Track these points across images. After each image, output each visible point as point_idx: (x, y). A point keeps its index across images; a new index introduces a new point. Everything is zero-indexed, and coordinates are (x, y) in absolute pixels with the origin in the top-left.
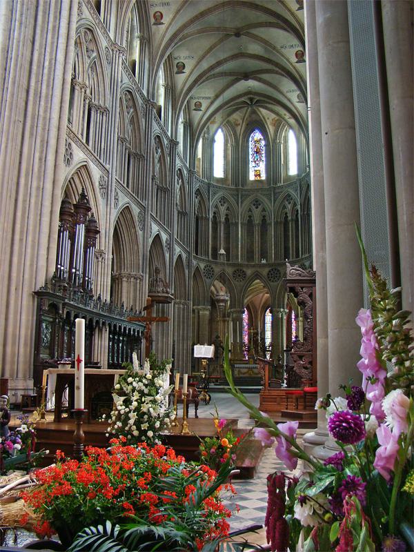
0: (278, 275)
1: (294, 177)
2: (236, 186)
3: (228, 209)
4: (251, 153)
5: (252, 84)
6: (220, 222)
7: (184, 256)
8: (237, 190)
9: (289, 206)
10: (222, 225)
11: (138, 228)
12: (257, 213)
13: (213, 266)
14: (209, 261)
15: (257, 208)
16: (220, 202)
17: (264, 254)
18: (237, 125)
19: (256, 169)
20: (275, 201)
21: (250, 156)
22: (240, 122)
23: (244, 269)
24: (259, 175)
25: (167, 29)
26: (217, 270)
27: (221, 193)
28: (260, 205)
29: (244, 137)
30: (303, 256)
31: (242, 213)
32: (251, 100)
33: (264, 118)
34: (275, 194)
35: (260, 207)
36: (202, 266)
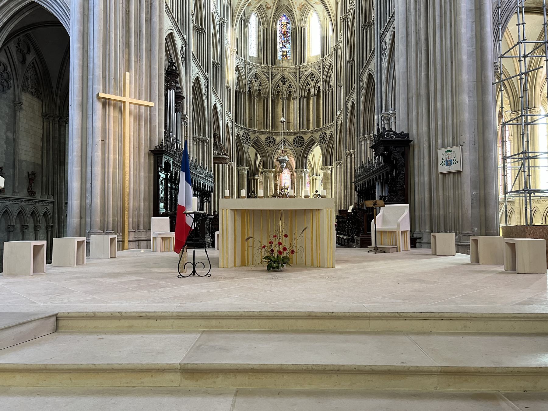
0: (302, 142)
1: (317, 56)
2: (267, 64)
3: (260, 84)
6: (254, 95)
7: (230, 124)
9: (312, 83)
11: (204, 97)
12: (284, 88)
14: (246, 129)
15: (284, 84)
18: (268, 8)
19: (283, 49)
21: (278, 38)
22: (271, 5)
23: (275, 137)
26: (253, 136)
27: (255, 70)
28: (287, 81)
29: (273, 20)
35: (287, 83)
36: (241, 133)
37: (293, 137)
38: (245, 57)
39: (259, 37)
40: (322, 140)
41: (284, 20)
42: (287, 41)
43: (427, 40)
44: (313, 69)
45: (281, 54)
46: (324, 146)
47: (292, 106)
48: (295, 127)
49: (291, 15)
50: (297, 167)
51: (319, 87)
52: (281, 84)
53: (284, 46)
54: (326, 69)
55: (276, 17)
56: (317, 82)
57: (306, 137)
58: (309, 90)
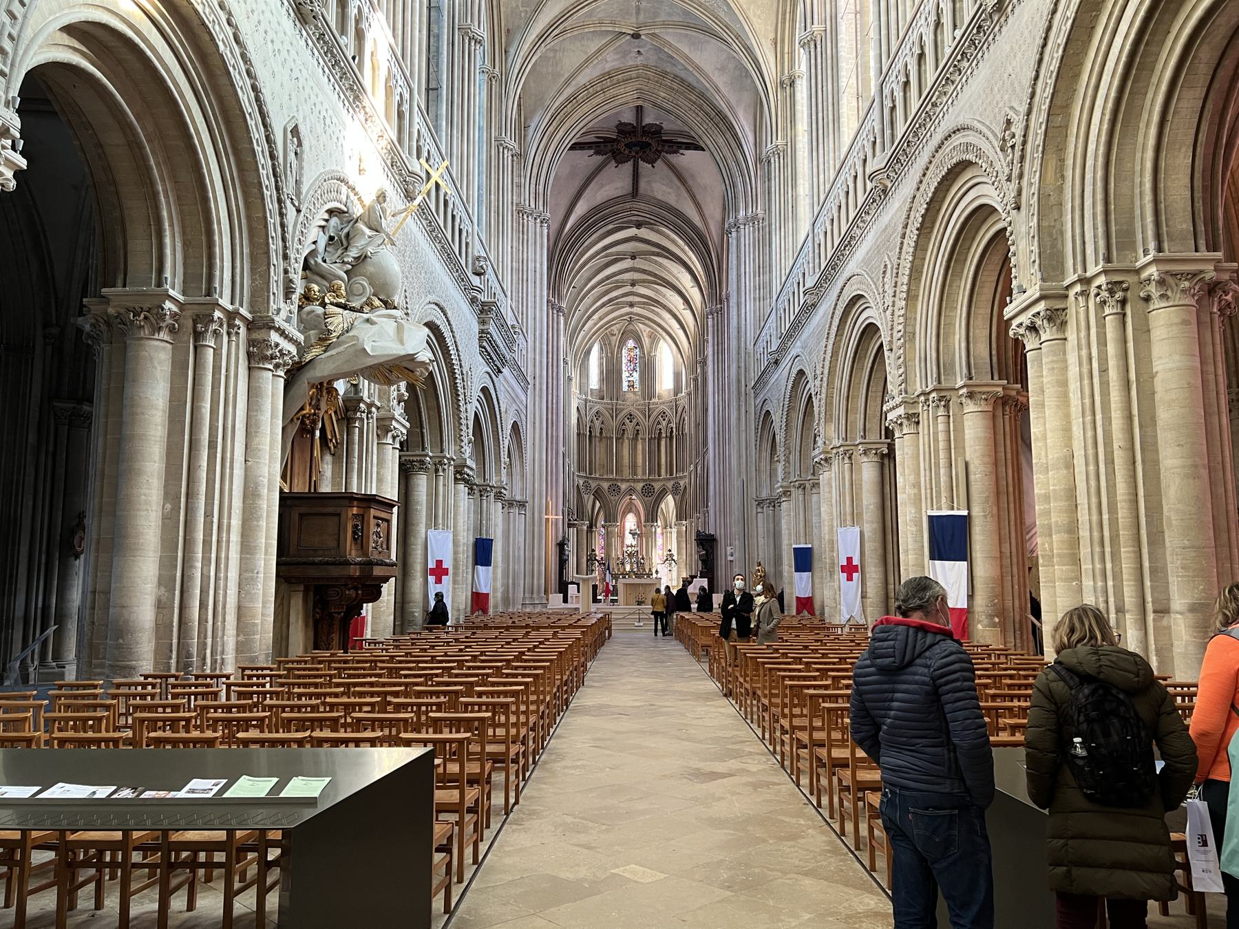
4: (624, 361)
9: (664, 423)
12: (630, 426)
26: (593, 485)
37: (641, 485)
38: (586, 394)
39: (601, 364)
40: (675, 491)
41: (631, 344)
46: (677, 497)
47: (640, 447)
48: (644, 473)
49: (638, 340)
50: (647, 521)
54: (680, 409)
55: (622, 343)
56: (669, 422)
57: (657, 486)
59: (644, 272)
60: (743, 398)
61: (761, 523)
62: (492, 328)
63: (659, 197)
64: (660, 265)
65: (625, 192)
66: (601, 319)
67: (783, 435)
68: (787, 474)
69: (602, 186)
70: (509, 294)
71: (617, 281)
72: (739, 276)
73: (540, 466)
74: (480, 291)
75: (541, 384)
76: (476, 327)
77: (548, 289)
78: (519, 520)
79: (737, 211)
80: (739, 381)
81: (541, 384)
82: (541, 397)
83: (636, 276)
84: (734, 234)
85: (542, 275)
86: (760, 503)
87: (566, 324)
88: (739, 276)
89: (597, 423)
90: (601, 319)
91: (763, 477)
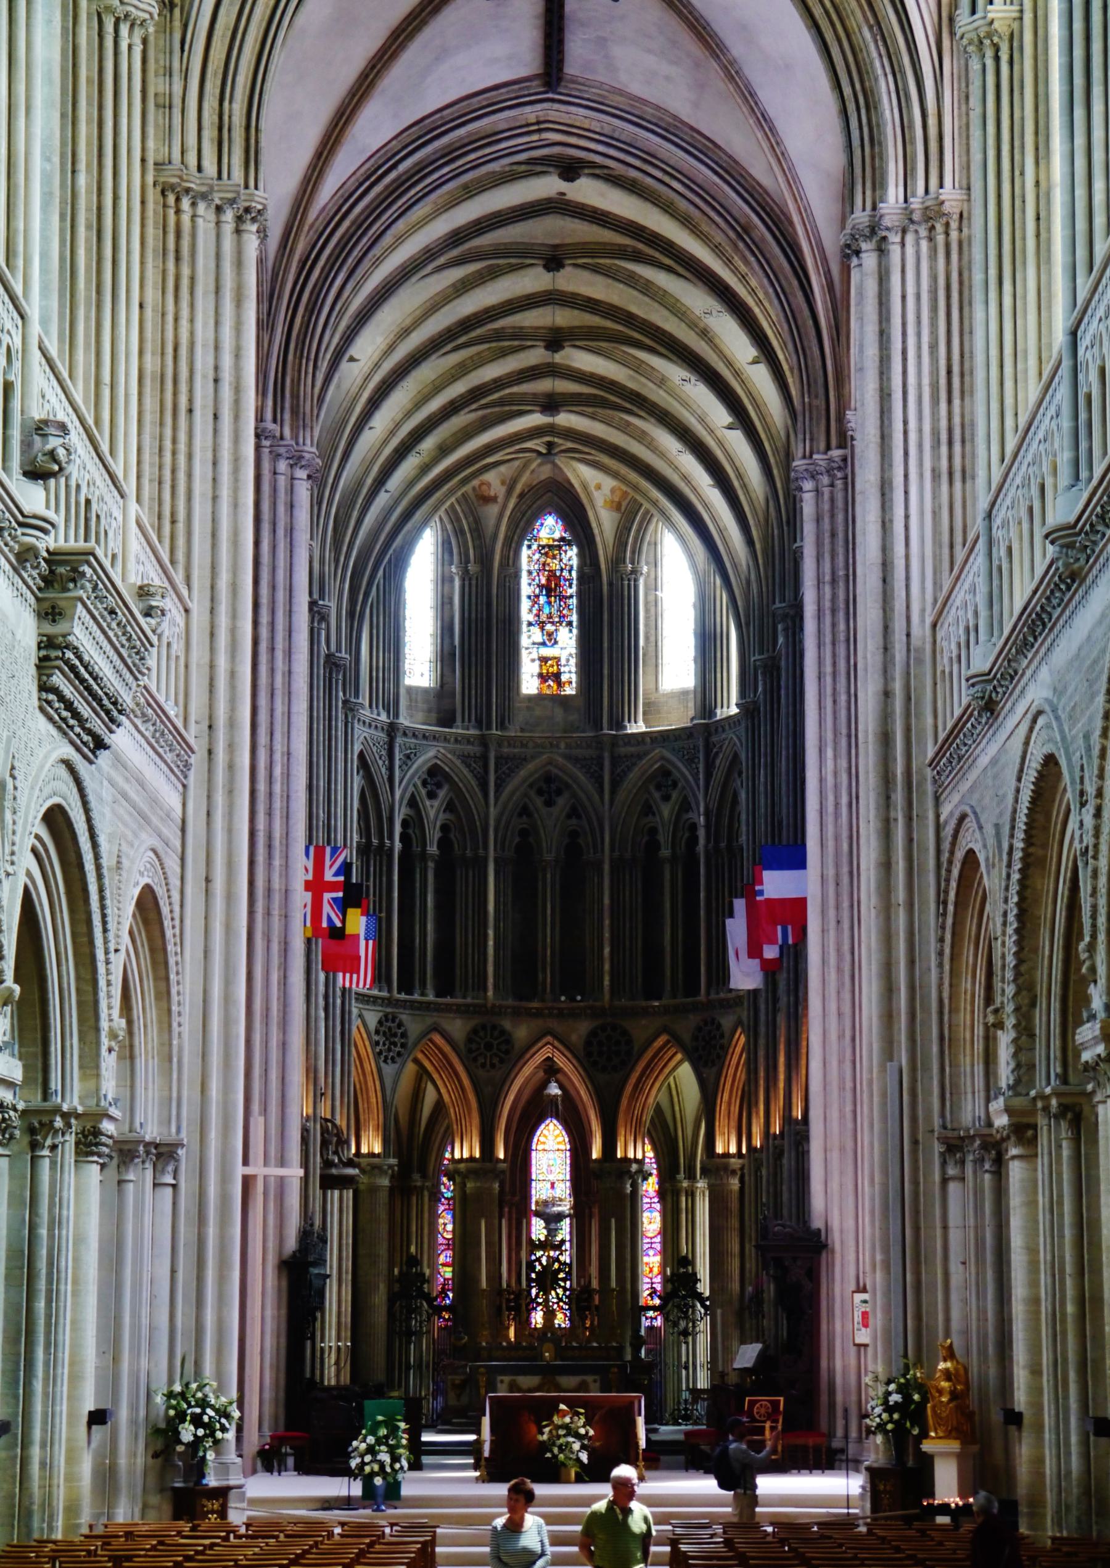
1: (685, 693)
2: (479, 724)
3: (450, 807)
4: (526, 589)
5: (565, 419)
8: (483, 741)
10: (431, 865)
12: (551, 821)
13: (404, 1017)
14: (389, 1002)
15: (549, 803)
16: (425, 783)
17: (575, 976)
18: (488, 500)
19: (546, 652)
20: (615, 785)
21: (525, 604)
23: (507, 1024)
24: (557, 676)
25: (367, 378)
27: (431, 753)
28: (559, 792)
30: (713, 996)
31: (498, 822)
32: (550, 445)
33: (585, 487)
34: (615, 760)
35: (561, 801)
36: (372, 1018)
38: (392, 707)
42: (562, 616)
43: (853, 1039)
44: (667, 754)
45: (535, 668)
51: (693, 827)
52: (539, 801)
53: (551, 639)
55: (521, 528)
58: (653, 831)
59: (591, 305)
60: (899, 797)
61: (959, 1207)
62: (83, 633)
63: (636, 88)
64: (647, 289)
65: (523, 73)
66: (444, 450)
67: (1011, 940)
68: (1024, 1069)
69: (443, 53)
70: (131, 488)
71: (498, 335)
72: (885, 395)
73: (227, 1022)
74: (43, 526)
75: (231, 747)
76: (26, 630)
77: (261, 391)
78: (150, 1204)
79: (878, 184)
80: (885, 739)
81: (231, 747)
82: (230, 792)
83: (563, 317)
84: (869, 260)
85: (237, 389)
86: (954, 1147)
87: (317, 502)
88: (885, 395)
89: (433, 810)
90: (444, 450)
91: (965, 1061)
